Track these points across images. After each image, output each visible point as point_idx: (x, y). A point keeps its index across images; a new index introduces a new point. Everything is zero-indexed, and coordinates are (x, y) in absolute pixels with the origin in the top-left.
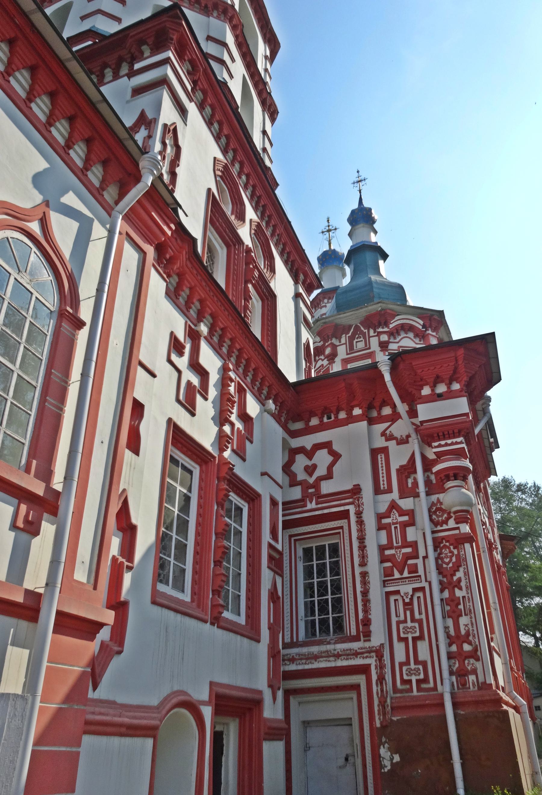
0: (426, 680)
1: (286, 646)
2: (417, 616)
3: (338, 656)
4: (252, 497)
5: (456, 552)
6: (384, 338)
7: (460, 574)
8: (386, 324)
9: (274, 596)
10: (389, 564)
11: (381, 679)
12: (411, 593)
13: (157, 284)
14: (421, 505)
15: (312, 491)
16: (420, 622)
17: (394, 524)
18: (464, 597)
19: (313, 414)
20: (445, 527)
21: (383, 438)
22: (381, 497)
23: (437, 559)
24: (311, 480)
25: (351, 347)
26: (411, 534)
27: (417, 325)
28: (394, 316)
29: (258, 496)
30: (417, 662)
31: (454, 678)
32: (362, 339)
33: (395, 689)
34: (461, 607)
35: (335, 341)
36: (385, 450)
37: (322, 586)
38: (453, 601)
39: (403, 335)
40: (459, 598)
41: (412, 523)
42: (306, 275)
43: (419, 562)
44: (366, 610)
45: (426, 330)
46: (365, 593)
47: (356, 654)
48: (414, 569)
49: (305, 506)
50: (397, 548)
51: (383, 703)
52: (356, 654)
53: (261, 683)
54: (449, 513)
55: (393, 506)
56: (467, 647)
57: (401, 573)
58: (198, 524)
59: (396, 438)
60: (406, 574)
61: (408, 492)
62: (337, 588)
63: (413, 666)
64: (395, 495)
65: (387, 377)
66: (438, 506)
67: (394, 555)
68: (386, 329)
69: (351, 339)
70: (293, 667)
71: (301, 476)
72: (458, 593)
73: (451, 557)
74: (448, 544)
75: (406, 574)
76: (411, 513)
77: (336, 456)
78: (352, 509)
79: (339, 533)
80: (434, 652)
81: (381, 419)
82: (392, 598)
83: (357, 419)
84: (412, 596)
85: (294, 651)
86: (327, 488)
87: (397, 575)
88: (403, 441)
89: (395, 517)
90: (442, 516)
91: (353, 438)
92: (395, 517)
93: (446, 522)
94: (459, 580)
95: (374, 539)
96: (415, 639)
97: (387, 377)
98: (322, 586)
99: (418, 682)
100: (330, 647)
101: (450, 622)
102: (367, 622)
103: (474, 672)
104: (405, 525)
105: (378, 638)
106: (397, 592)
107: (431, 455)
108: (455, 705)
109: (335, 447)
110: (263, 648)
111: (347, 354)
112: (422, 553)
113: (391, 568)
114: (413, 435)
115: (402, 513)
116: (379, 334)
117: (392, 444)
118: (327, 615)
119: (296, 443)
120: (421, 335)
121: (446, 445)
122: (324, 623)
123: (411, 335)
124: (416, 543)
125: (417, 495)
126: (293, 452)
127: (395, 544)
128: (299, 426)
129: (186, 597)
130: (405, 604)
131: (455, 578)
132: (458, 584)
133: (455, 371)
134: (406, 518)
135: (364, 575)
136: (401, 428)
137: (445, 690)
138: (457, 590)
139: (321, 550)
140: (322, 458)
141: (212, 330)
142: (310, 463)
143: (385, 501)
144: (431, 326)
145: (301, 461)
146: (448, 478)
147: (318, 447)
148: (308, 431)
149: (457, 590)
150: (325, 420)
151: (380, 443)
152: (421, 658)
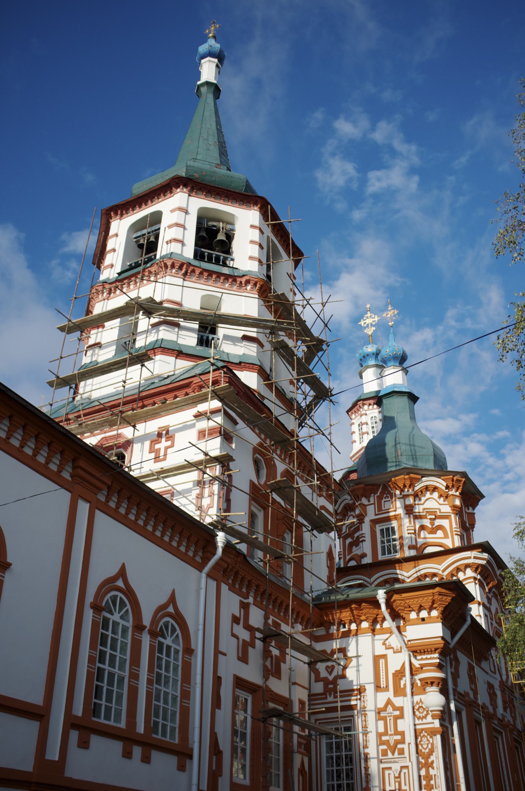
5: (431, 741)
7: (432, 758)
10: (385, 747)
12: (399, 770)
17: (389, 716)
18: (435, 775)
20: (424, 721)
21: (384, 646)
24: (331, 678)
27: (441, 486)
32: (389, 499)
34: (432, 782)
35: (364, 501)
36: (384, 656)
39: (428, 495)
40: (432, 776)
41: (401, 716)
43: (405, 747)
48: (402, 752)
49: (326, 698)
50: (391, 735)
54: (427, 711)
55: (389, 702)
57: (393, 754)
59: (392, 648)
61: (399, 691)
64: (390, 694)
66: (420, 705)
67: (388, 741)
71: (324, 674)
72: (432, 772)
73: (428, 744)
74: (426, 734)
76: (401, 709)
79: (351, 720)
81: (383, 631)
82: (387, 772)
83: (365, 631)
84: (400, 772)
87: (390, 755)
90: (422, 713)
93: (425, 717)
94: (433, 762)
104: (396, 718)
106: (390, 768)
107: (416, 663)
111: (376, 515)
112: (407, 740)
113: (386, 750)
114: (405, 650)
115: (395, 708)
116: (405, 497)
117: (389, 653)
121: (427, 659)
125: (405, 695)
127: (389, 733)
130: (395, 778)
131: (430, 760)
132: (431, 765)
133: (433, 602)
134: (397, 713)
138: (430, 769)
141: (255, 599)
143: (382, 698)
149: (430, 769)
151: (380, 650)
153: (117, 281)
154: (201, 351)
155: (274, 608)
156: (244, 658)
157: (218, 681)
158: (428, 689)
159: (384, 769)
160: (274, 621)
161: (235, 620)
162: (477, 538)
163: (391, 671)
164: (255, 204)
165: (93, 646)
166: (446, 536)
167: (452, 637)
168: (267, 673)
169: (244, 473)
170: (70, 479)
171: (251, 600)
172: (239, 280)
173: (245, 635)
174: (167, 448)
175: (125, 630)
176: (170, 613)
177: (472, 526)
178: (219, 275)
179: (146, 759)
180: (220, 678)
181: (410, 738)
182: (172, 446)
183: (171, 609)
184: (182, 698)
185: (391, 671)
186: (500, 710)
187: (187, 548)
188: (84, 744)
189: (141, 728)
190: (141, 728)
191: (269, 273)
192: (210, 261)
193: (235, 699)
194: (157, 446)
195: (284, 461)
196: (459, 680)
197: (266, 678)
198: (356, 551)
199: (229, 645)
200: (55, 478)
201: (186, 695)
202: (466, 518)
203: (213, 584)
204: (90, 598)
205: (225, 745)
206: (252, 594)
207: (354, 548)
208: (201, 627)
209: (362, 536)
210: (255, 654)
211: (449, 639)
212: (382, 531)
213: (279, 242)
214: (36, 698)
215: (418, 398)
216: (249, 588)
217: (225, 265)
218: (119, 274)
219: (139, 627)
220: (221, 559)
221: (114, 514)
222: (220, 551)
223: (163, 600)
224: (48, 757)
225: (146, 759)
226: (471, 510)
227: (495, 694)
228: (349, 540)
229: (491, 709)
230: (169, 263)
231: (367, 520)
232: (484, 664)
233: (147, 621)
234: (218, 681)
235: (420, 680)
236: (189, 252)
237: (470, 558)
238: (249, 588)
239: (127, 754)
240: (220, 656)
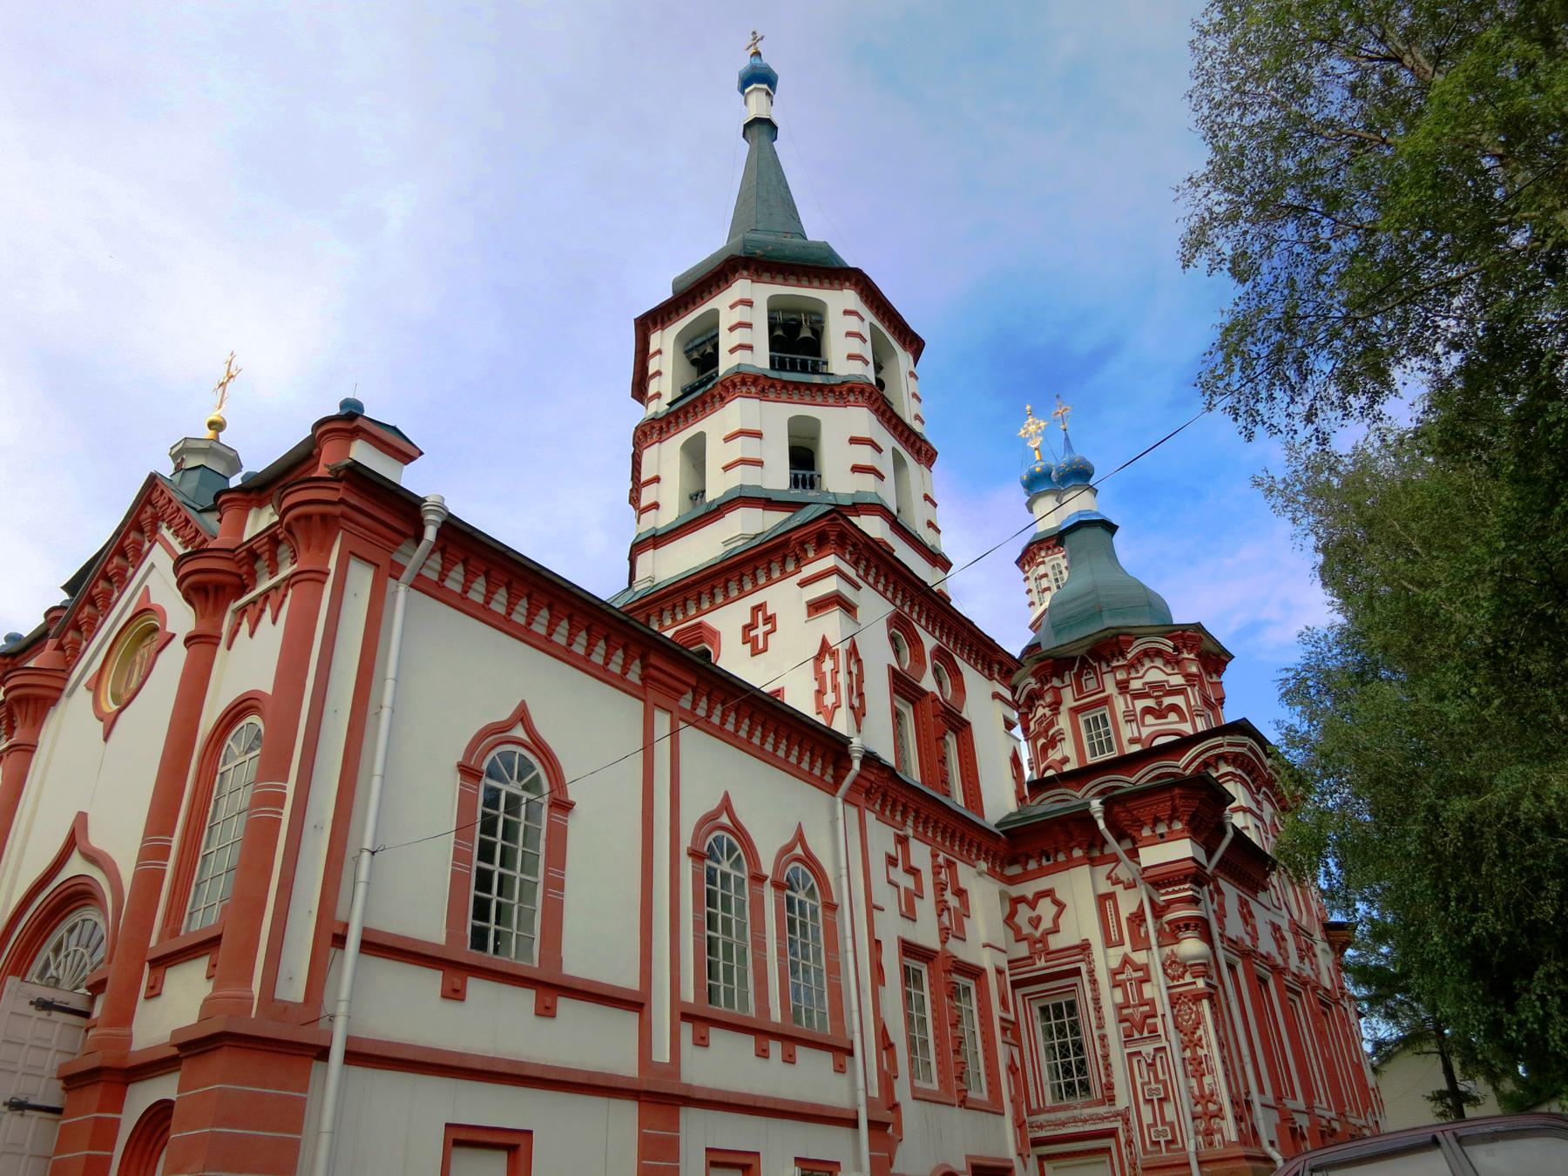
0: (1173, 1141)
1: (1031, 1113)
2: (1161, 1076)
3: (1085, 1121)
4: (976, 973)
6: (1121, 676)
7: (1200, 1032)
8: (1123, 654)
9: (1012, 1069)
11: (1129, 1142)
13: (870, 817)
14: (1153, 958)
15: (1039, 944)
16: (1164, 1083)
19: (1028, 857)
20: (1181, 982)
22: (1111, 951)
23: (1175, 1018)
24: (1038, 934)
25: (1080, 690)
26: (1148, 991)
28: (1130, 643)
29: (984, 970)
30: (1164, 1122)
31: (1200, 1138)
33: (1145, 1150)
35: (1056, 682)
37: (1063, 1046)
38: (1197, 1061)
39: (1148, 664)
42: (1001, 664)
43: (1159, 1020)
44: (1108, 1075)
45: (1180, 653)
46: (1106, 1057)
47: (1103, 1119)
48: (1154, 1030)
51: (1133, 1166)
52: (1103, 1119)
53: (1011, 1152)
55: (1126, 961)
56: (1212, 1107)
58: (934, 1019)
60: (1146, 1034)
61: (1140, 943)
62: (1079, 1048)
63: (1160, 1128)
64: (1127, 947)
65: (1101, 825)
68: (1122, 662)
69: (1078, 676)
70: (1042, 1134)
71: (1027, 929)
75: (1146, 1034)
76: (1145, 968)
77: (1061, 906)
78: (1083, 967)
80: (1181, 1111)
85: (1042, 1118)
86: (1055, 942)
87: (1137, 1036)
88: (1130, 886)
89: (1129, 973)
91: (1078, 887)
92: (1129, 973)
93: (1182, 976)
95: (1110, 998)
96: (1160, 1100)
97: (1101, 825)
98: (1063, 1046)
99: (1167, 1142)
100: (1076, 1113)
101: (1194, 1082)
102: (1110, 1086)
103: (1220, 1130)
105: (1123, 1100)
108: (1200, 1163)
109: (1059, 896)
110: (1008, 1121)
112: (1159, 1012)
114: (1139, 882)
117: (1119, 889)
118: (1074, 1073)
119: (1016, 891)
120: (1174, 661)
121: (1174, 892)
122: (1070, 1085)
123: (1159, 662)
124: (1153, 1000)
126: (1016, 901)
128: (1015, 870)
129: (935, 1086)
130: (1149, 1065)
132: (1198, 1044)
133: (1174, 809)
135: (1103, 1038)
136: (1124, 871)
137: (1191, 1147)
139: (1058, 1007)
140: (1046, 908)
141: (915, 828)
142: (1034, 914)
144: (1185, 646)
145: (1024, 913)
146: (1179, 927)
147: (1040, 895)
148: (1026, 877)
150: (1044, 863)
151: (1105, 887)
152: (1168, 1119)
153: (668, 415)
154: (799, 495)
155: (943, 839)
156: (909, 914)
157: (876, 945)
158: (1181, 935)
159: (1130, 1055)
160: (947, 860)
161: (892, 861)
162: (1229, 715)
163: (1124, 915)
164: (848, 279)
165: (697, 907)
166: (1183, 719)
167: (1209, 856)
168: (945, 933)
169: (879, 656)
170: (639, 683)
171: (910, 832)
172: (837, 390)
173: (907, 882)
174: (766, 634)
175: (739, 883)
176: (798, 853)
177: (1221, 701)
178: (809, 387)
179: (789, 1059)
180: (878, 942)
181: (1163, 1006)
182: (773, 630)
183: (799, 851)
184: (829, 973)
185: (1124, 915)
186: (1294, 962)
187: (812, 764)
188: (701, 1041)
189: (776, 1015)
190: (776, 1015)
191: (880, 376)
192: (793, 369)
193: (906, 969)
194: (753, 633)
195: (932, 634)
196: (1226, 921)
197: (944, 942)
198: (1055, 755)
199: (884, 895)
200: (618, 682)
201: (835, 968)
202: (1209, 691)
203: (853, 812)
204: (686, 841)
205: (898, 1035)
206: (910, 822)
207: (1050, 752)
208: (844, 872)
209: (1060, 732)
210: (926, 908)
211: (1203, 860)
212: (1087, 722)
213: (888, 328)
214: (627, 979)
215: (1116, 527)
216: (904, 815)
217: (815, 371)
218: (670, 404)
219: (758, 879)
220: (859, 775)
221: (704, 725)
222: (856, 765)
223: (788, 838)
224: (655, 1058)
225: (789, 1059)
226: (1215, 679)
227: (1283, 939)
228: (1042, 741)
229: (1279, 961)
230: (737, 380)
231: (1063, 708)
232: (1262, 896)
233: (767, 868)
234: (876, 945)
235: (1169, 923)
236: (760, 359)
237: (1221, 745)
238: (904, 815)
239: (763, 1053)
240: (876, 913)
